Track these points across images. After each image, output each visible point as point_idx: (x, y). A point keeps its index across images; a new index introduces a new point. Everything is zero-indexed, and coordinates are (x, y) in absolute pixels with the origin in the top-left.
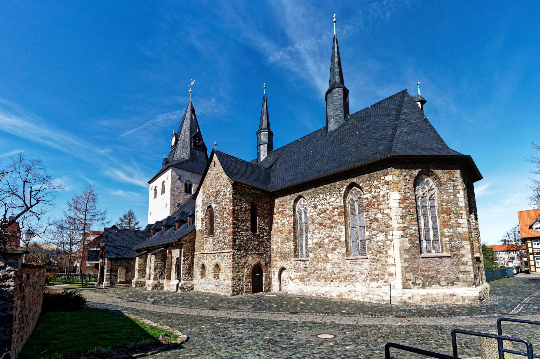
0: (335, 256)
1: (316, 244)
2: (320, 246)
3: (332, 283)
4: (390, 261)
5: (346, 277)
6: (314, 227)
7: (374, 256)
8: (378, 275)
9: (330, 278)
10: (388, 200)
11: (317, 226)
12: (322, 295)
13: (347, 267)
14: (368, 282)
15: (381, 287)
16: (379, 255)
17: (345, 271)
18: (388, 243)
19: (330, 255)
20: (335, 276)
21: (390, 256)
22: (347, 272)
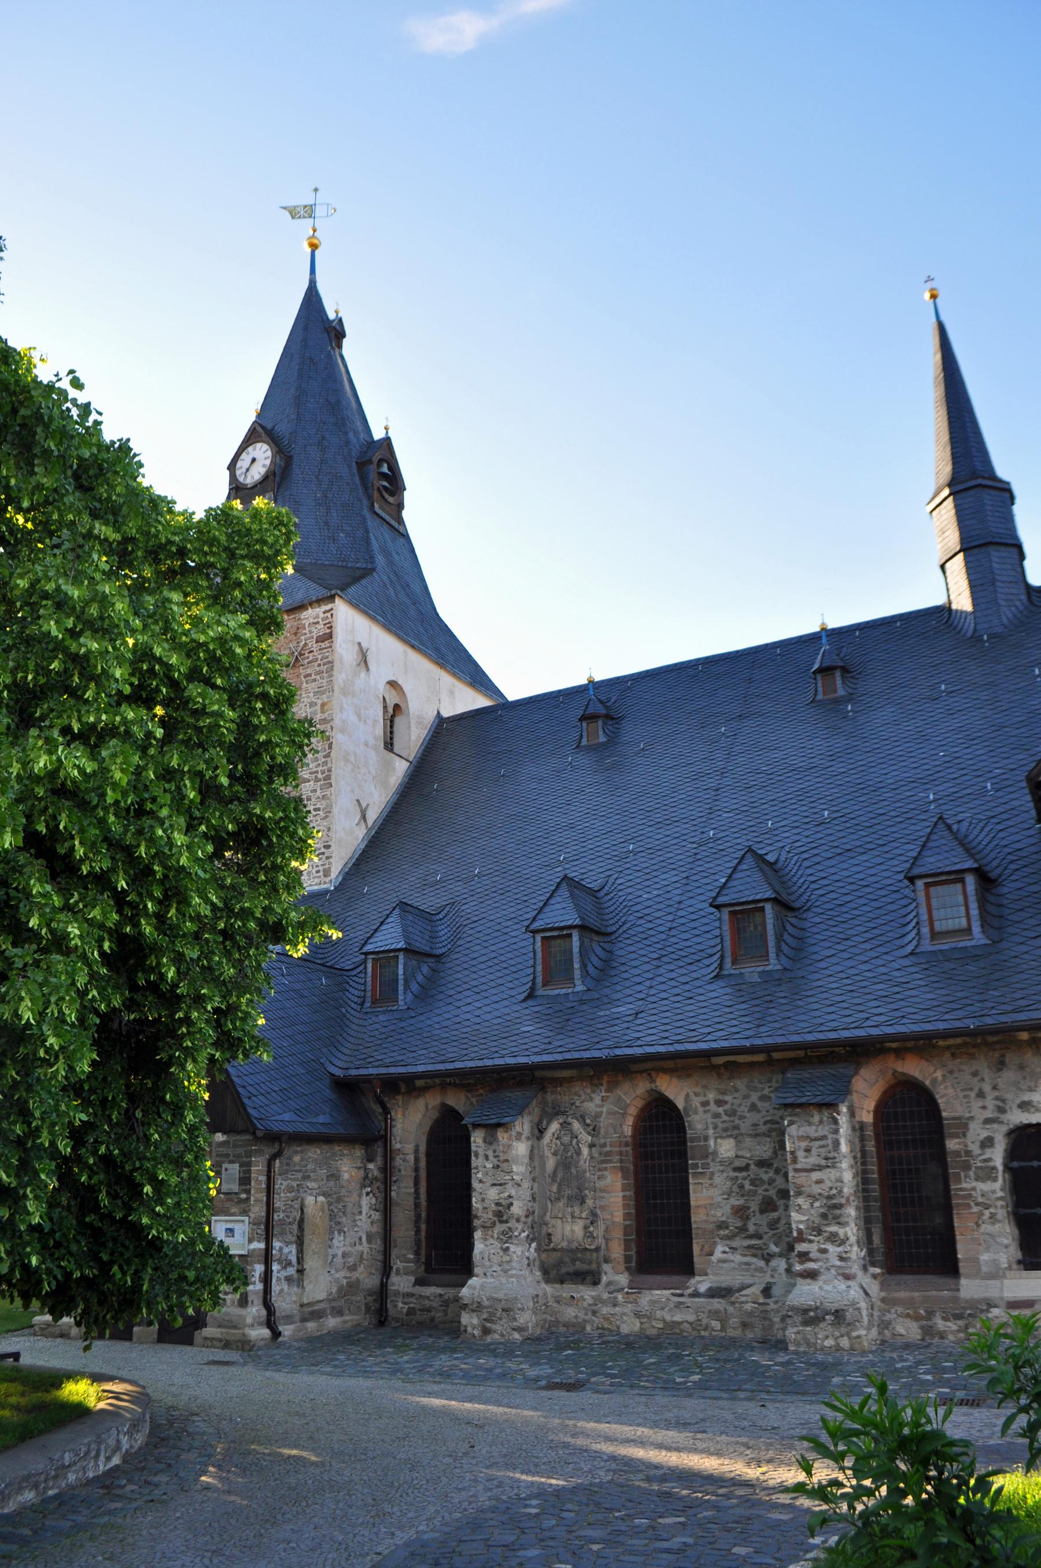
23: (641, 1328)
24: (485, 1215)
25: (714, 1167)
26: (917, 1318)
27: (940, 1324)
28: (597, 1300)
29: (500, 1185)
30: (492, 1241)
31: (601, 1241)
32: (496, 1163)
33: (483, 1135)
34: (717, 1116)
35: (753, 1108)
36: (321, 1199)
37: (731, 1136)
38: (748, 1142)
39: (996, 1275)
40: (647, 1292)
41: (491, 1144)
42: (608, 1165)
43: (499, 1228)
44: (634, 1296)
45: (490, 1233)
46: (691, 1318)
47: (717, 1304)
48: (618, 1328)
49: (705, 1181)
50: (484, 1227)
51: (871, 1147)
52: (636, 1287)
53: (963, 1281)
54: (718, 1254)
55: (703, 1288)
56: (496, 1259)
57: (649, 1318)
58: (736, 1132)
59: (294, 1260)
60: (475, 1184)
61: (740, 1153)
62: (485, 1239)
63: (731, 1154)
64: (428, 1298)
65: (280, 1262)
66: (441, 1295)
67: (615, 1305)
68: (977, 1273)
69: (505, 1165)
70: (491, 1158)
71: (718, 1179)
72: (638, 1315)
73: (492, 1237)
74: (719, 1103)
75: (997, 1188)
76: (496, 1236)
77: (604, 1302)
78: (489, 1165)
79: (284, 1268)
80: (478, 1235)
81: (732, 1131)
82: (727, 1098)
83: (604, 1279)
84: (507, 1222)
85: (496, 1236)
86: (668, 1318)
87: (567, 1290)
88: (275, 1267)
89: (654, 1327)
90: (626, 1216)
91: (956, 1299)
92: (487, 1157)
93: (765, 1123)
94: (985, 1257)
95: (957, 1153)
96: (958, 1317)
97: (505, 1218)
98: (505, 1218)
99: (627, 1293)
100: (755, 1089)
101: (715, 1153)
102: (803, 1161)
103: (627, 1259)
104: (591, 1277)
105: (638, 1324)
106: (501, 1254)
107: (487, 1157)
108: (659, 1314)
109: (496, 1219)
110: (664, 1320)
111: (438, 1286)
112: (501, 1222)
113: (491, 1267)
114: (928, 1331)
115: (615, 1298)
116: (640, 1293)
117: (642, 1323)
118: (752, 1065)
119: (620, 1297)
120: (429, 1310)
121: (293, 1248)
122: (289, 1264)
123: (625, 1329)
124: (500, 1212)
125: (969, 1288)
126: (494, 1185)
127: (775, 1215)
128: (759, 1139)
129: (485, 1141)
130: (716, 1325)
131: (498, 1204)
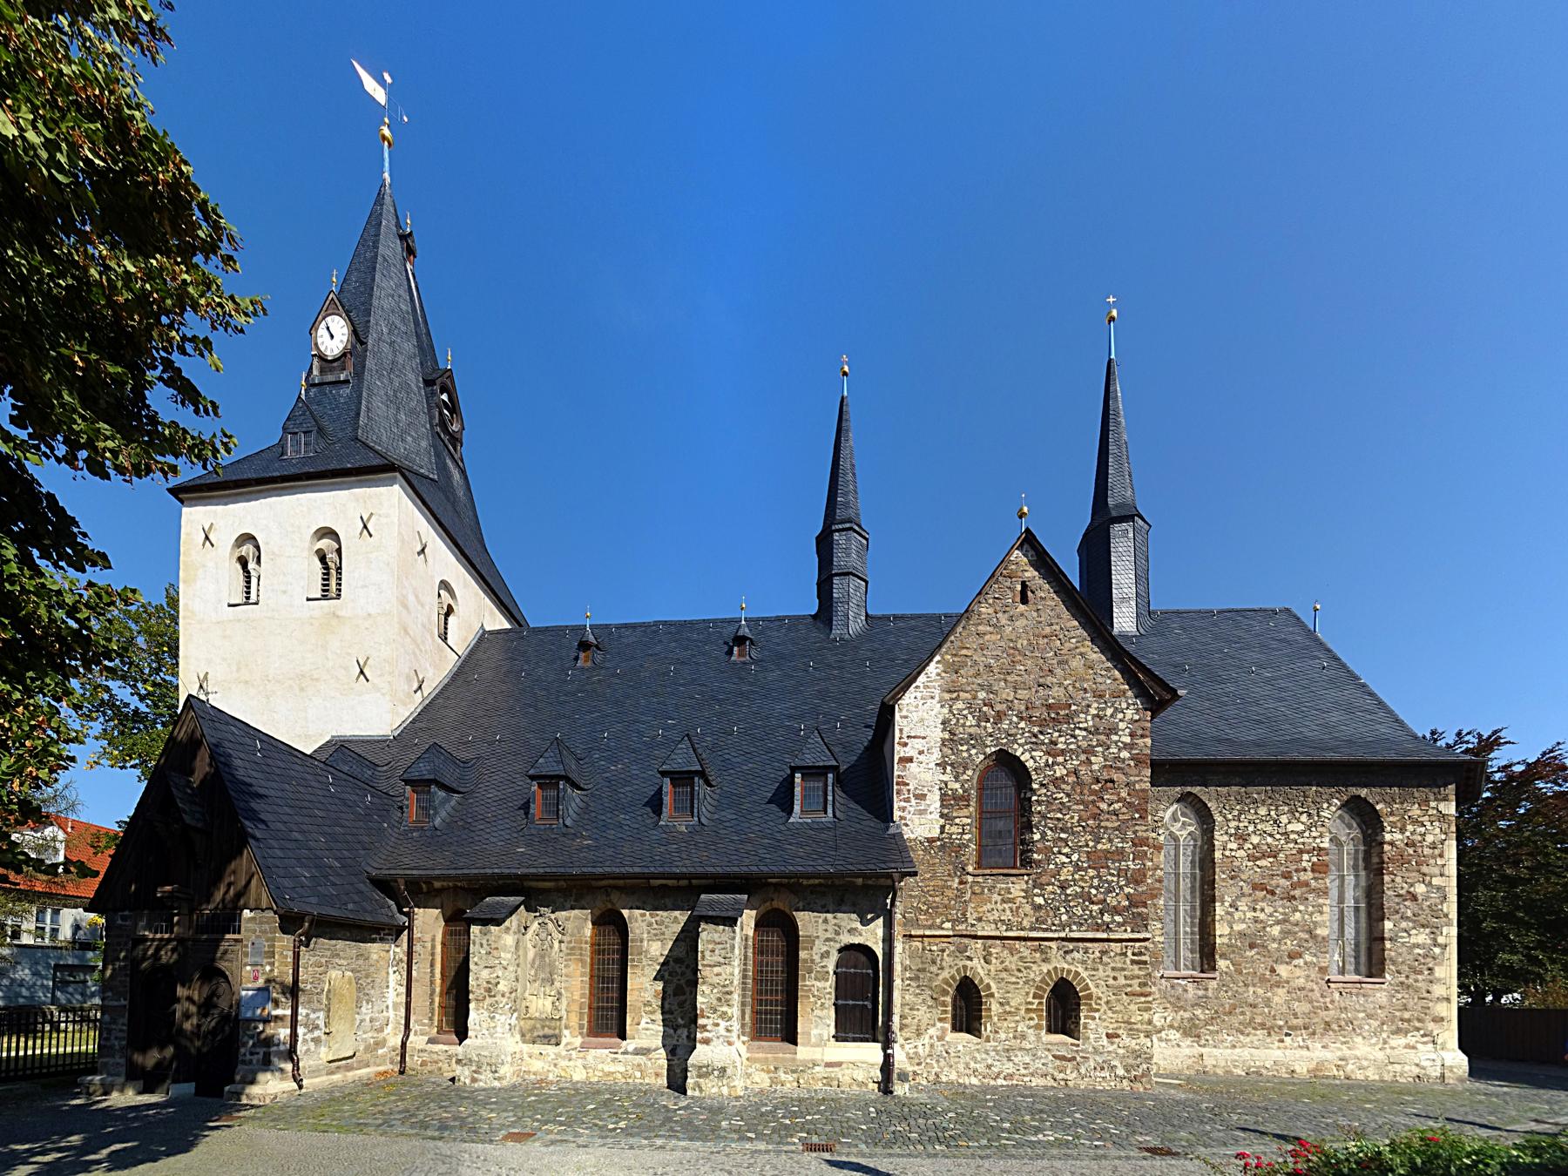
0: (1298, 972)
1: (1242, 935)
2: (1253, 941)
3: (1287, 1039)
4: (1439, 990)
5: (1327, 1024)
6: (1236, 890)
7: (1403, 979)
8: (1409, 1021)
9: (1280, 1028)
10: (1441, 856)
11: (1247, 890)
12: (1264, 1072)
13: (1332, 1002)
14: (1384, 1035)
15: (1414, 1048)
16: (1413, 976)
17: (1327, 1009)
18: (1437, 950)
19: (1283, 970)
20: (1299, 1022)
21: (1439, 980)
22: (1332, 1012)
26: (768, 1072)
27: (783, 1077)
28: (558, 1055)
31: (563, 1013)
36: (348, 974)
39: (821, 1043)
43: (488, 1001)
49: (638, 971)
51: (750, 955)
52: (585, 1047)
53: (799, 1048)
54: (643, 1024)
55: (630, 1049)
56: (485, 1025)
59: (322, 1025)
60: (472, 966)
65: (306, 1026)
68: (808, 1044)
69: (495, 953)
75: (829, 984)
77: (564, 1058)
79: (311, 1031)
80: (472, 1006)
83: (564, 1041)
87: (537, 1048)
88: (301, 1030)
90: (582, 996)
91: (794, 1060)
94: (814, 1032)
95: (805, 961)
96: (794, 1072)
102: (709, 959)
103: (581, 1027)
104: (553, 1039)
114: (773, 1081)
118: (679, 888)
121: (322, 1015)
122: (317, 1027)
123: (576, 1078)
125: (803, 1052)
127: (682, 998)
130: (638, 1074)
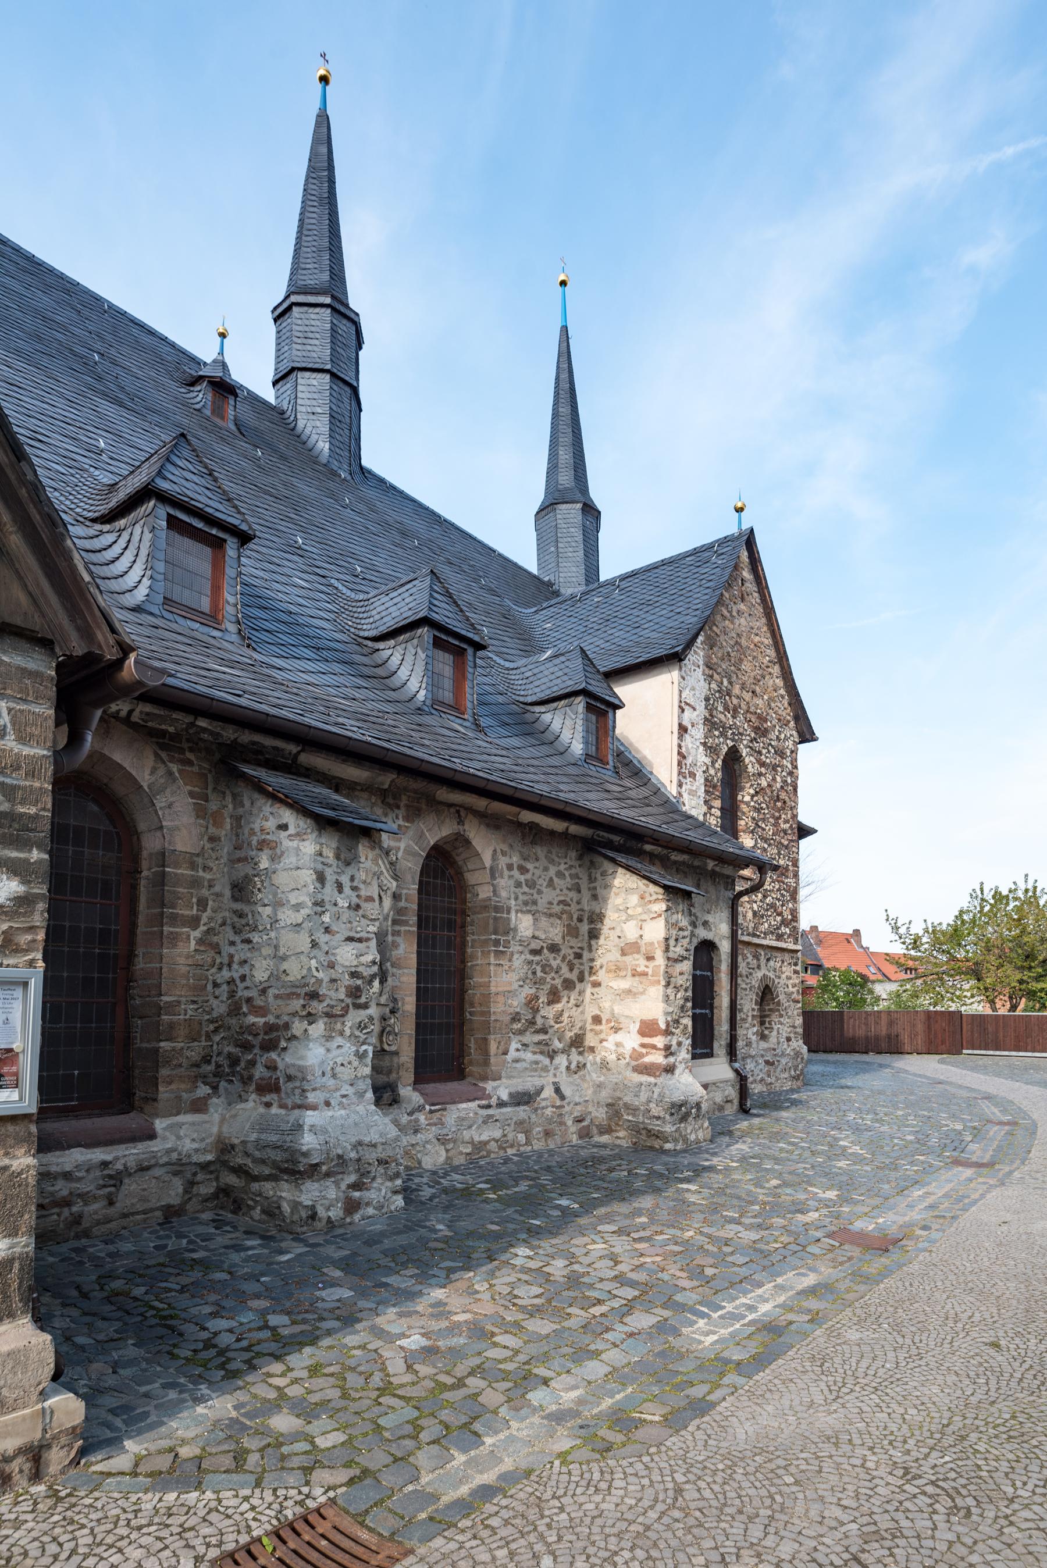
23: (448, 1158)
24: (332, 993)
25: (515, 948)
29: (360, 940)
30: (339, 1041)
32: (355, 900)
33: (334, 845)
34: (518, 885)
35: (551, 883)
37: (529, 912)
38: (544, 921)
40: (453, 1107)
41: (348, 864)
42: (403, 928)
44: (438, 1114)
45: (339, 1026)
46: (498, 1134)
47: (522, 1112)
48: (419, 1163)
50: (328, 1015)
56: (346, 1074)
57: (455, 1142)
58: (534, 908)
61: (537, 934)
62: (329, 1038)
63: (529, 933)
64: (67, 1176)
66: (105, 1164)
67: (416, 1131)
70: (347, 890)
71: (518, 961)
72: (442, 1140)
73: (341, 1033)
74: (523, 870)
76: (348, 1032)
78: (343, 903)
81: (529, 906)
82: (529, 866)
84: (365, 1006)
85: (348, 1032)
86: (477, 1139)
89: (461, 1153)
92: (340, 887)
93: (560, 902)
97: (363, 1000)
98: (363, 1000)
99: (431, 1112)
100: (552, 862)
101: (515, 930)
105: (443, 1153)
106: (356, 1063)
107: (340, 887)
108: (466, 1135)
109: (349, 1001)
110: (472, 1142)
111: (87, 1146)
112: (357, 1006)
113: (337, 1090)
115: (417, 1120)
116: (445, 1109)
117: (447, 1151)
119: (422, 1118)
120: (66, 1203)
124: (358, 988)
126: (350, 939)
128: (552, 920)
129: (338, 857)
131: (354, 975)
